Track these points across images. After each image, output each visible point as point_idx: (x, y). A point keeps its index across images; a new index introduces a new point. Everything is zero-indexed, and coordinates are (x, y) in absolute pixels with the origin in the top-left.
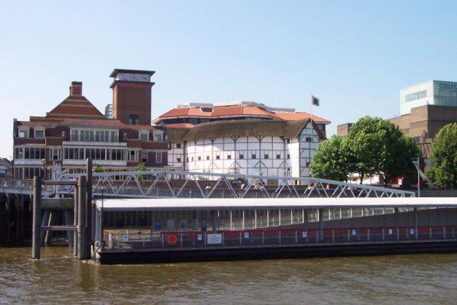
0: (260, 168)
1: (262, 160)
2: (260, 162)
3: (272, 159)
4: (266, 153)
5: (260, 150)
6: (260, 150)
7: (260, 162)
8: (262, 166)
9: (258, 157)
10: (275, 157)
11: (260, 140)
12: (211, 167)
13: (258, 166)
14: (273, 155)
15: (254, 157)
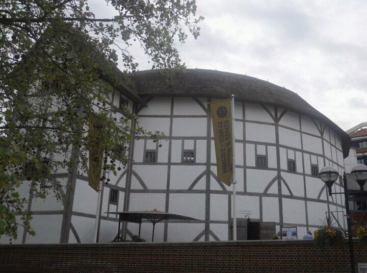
0: (280, 196)
1: (282, 174)
2: (279, 178)
3: (304, 174)
4: (291, 157)
5: (278, 145)
6: (278, 145)
7: (279, 178)
8: (285, 191)
9: (272, 163)
10: (308, 171)
11: (277, 120)
12: (122, 184)
13: (274, 189)
14: (304, 164)
15: (262, 163)
